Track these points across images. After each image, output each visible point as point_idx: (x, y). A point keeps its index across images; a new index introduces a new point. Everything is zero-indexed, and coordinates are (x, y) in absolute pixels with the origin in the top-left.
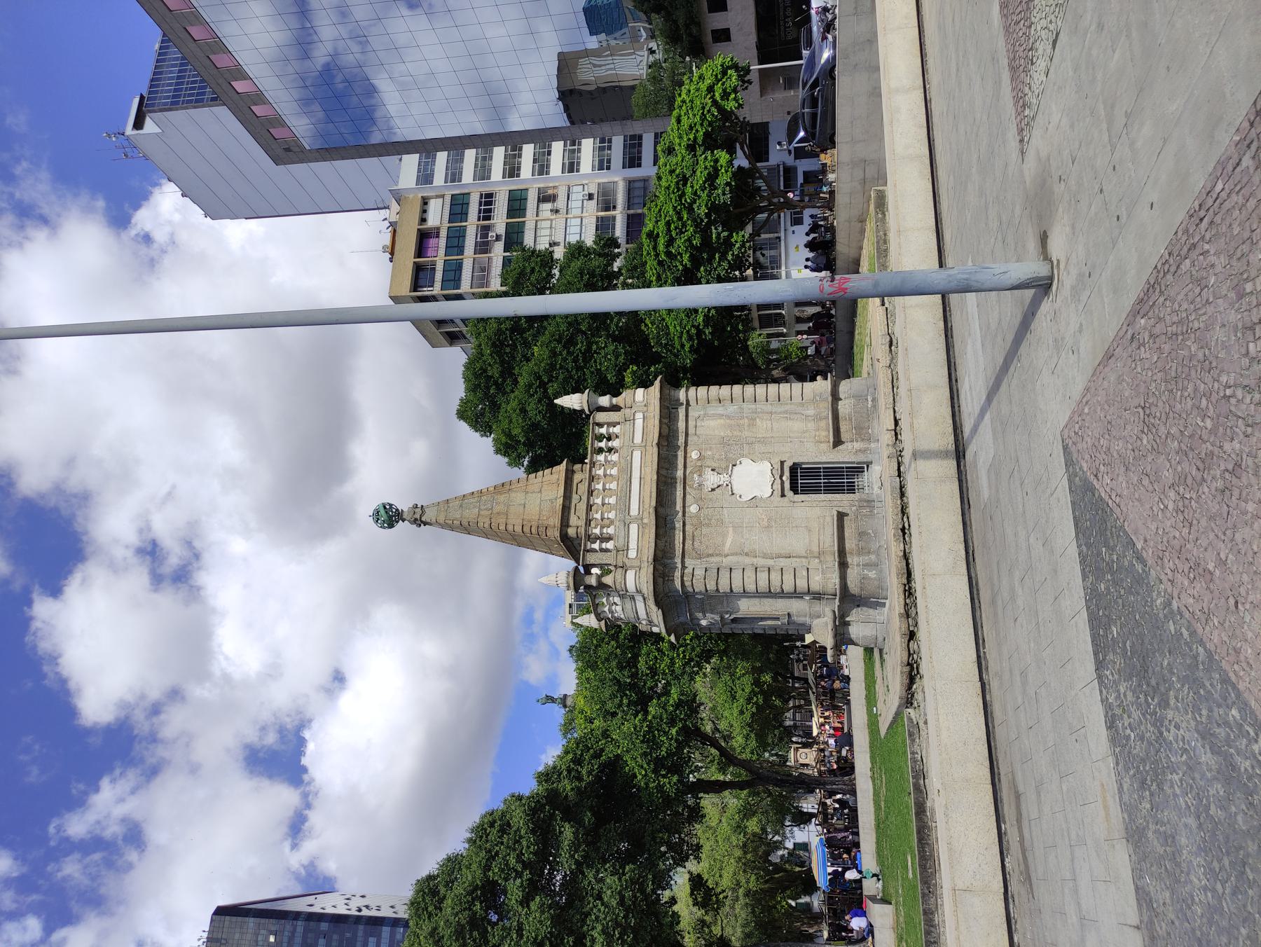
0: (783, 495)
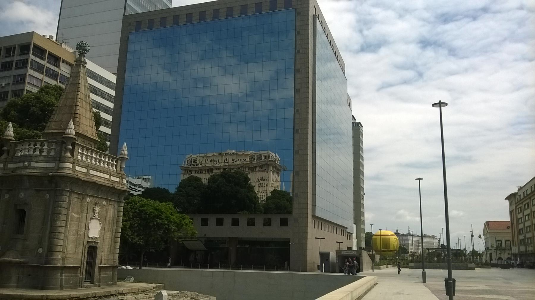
0: (88, 242)
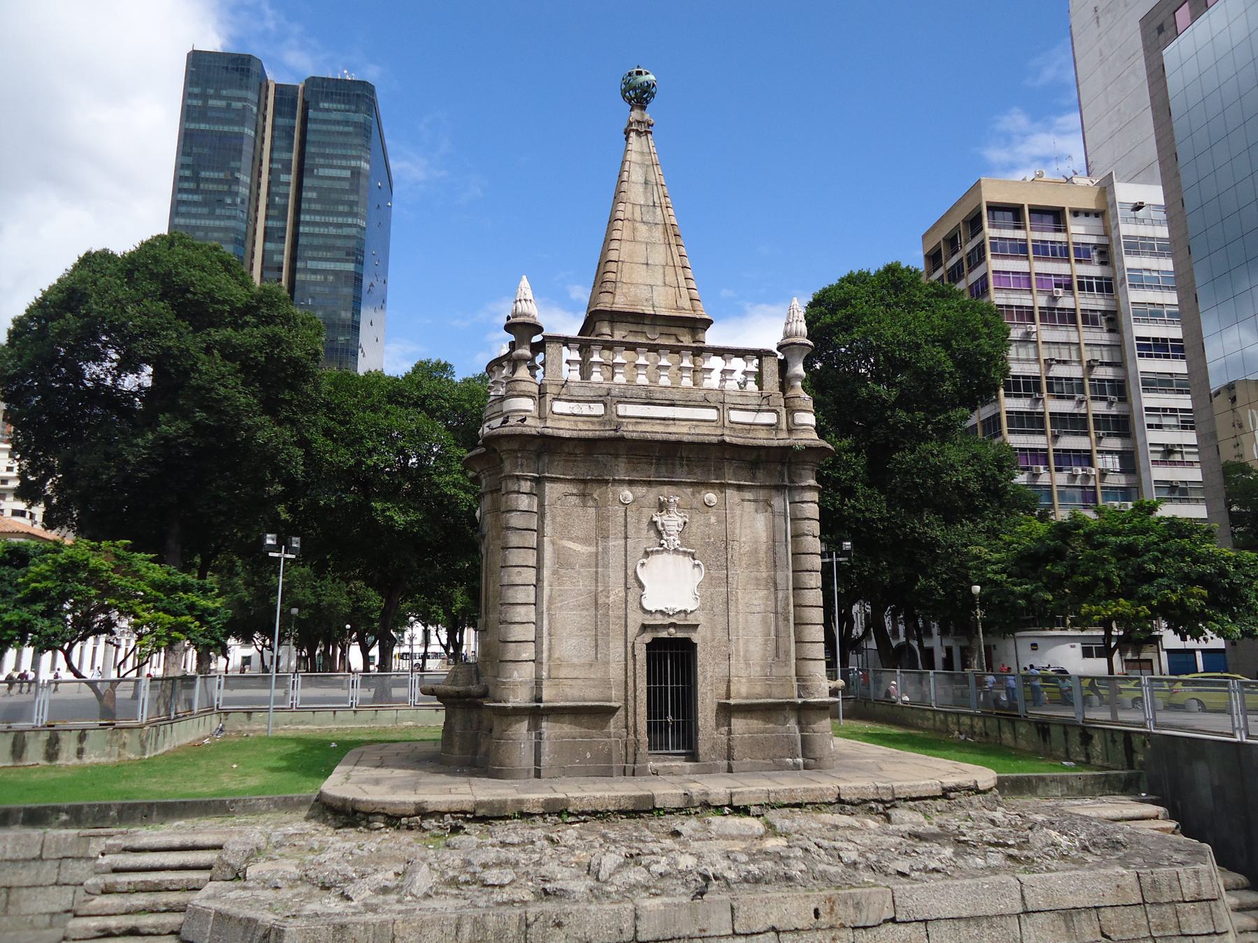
0: (644, 628)
